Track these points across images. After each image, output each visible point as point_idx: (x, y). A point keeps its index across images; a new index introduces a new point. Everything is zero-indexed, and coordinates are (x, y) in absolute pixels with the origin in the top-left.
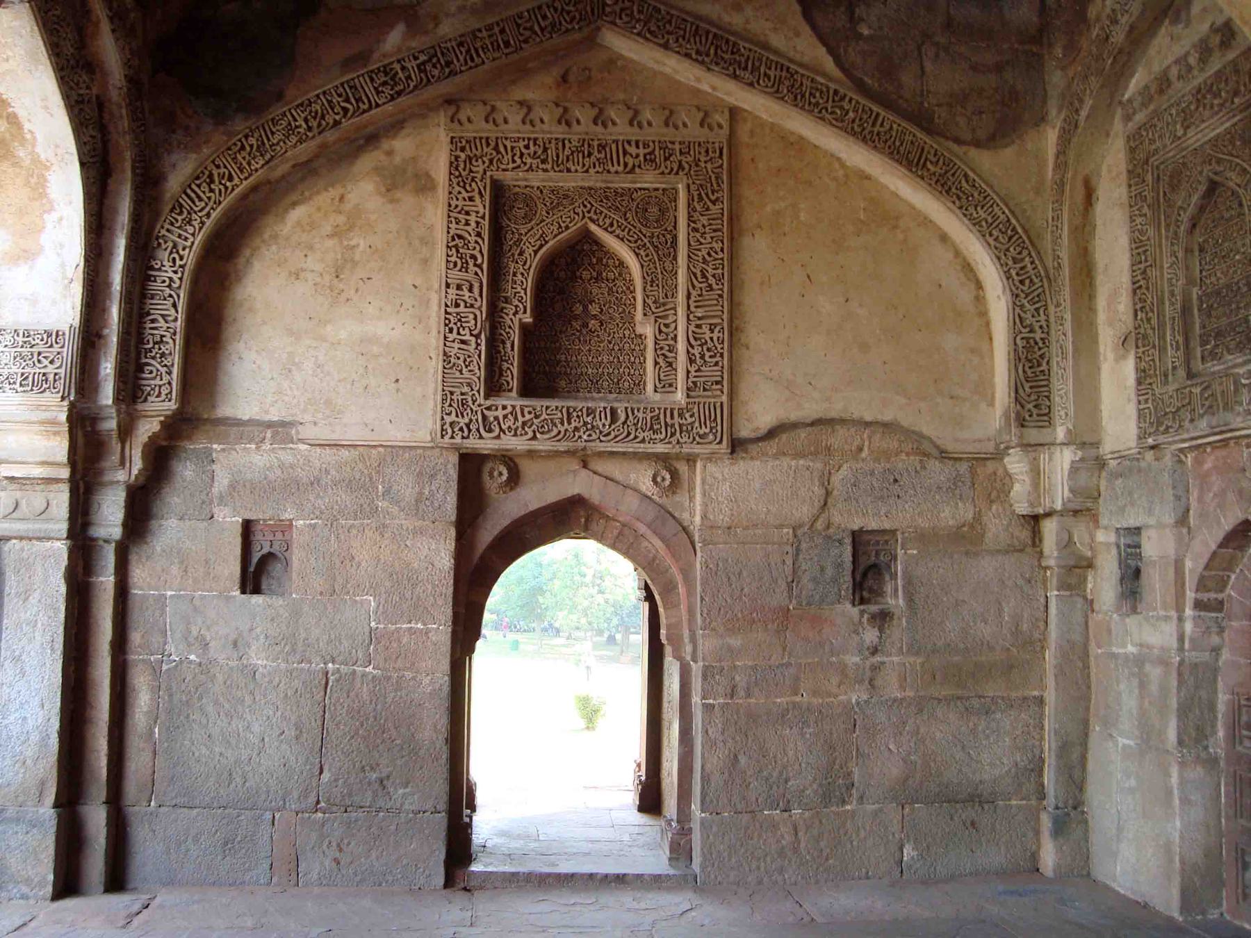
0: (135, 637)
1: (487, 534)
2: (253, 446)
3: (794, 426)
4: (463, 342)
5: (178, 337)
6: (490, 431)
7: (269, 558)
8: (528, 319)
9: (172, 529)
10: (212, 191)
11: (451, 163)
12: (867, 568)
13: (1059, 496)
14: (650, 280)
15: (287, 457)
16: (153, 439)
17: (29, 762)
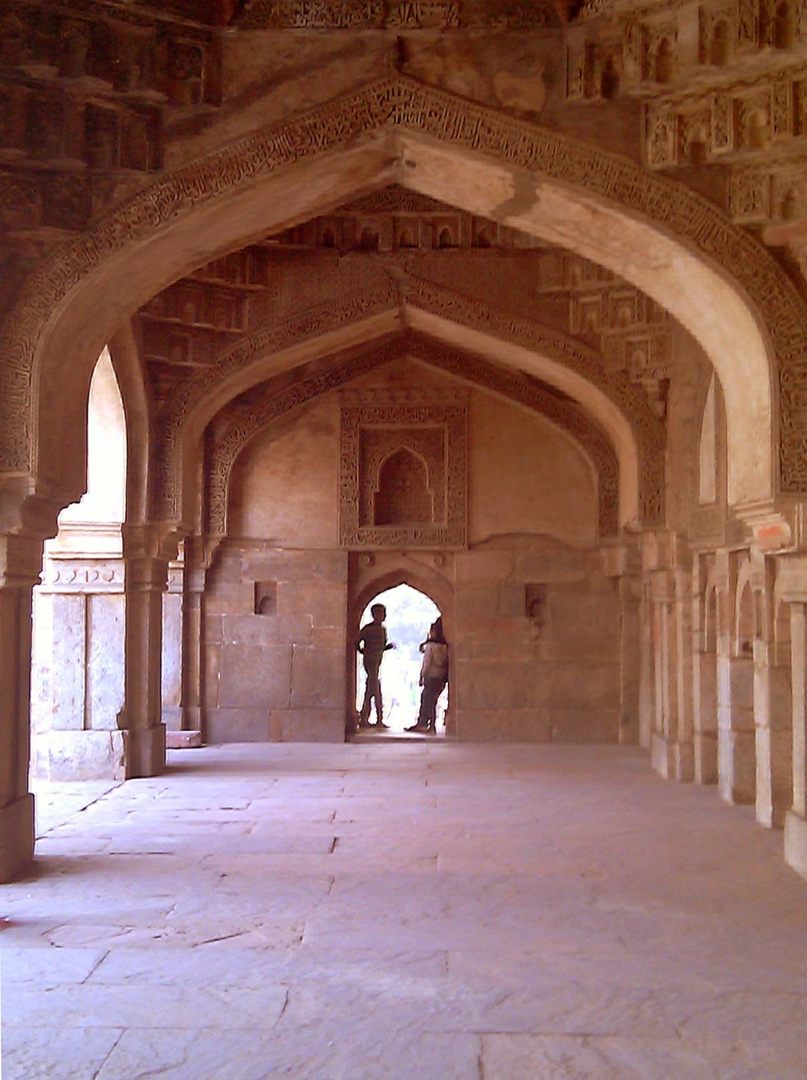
0: (209, 634)
1: (361, 587)
2: (258, 550)
3: (499, 536)
4: (349, 502)
5: (226, 505)
6: (361, 541)
7: (266, 599)
8: (378, 490)
9: (224, 587)
10: (237, 439)
11: (341, 419)
12: (533, 602)
13: (620, 568)
14: (432, 471)
15: (273, 554)
16: (217, 548)
17: (169, 688)
